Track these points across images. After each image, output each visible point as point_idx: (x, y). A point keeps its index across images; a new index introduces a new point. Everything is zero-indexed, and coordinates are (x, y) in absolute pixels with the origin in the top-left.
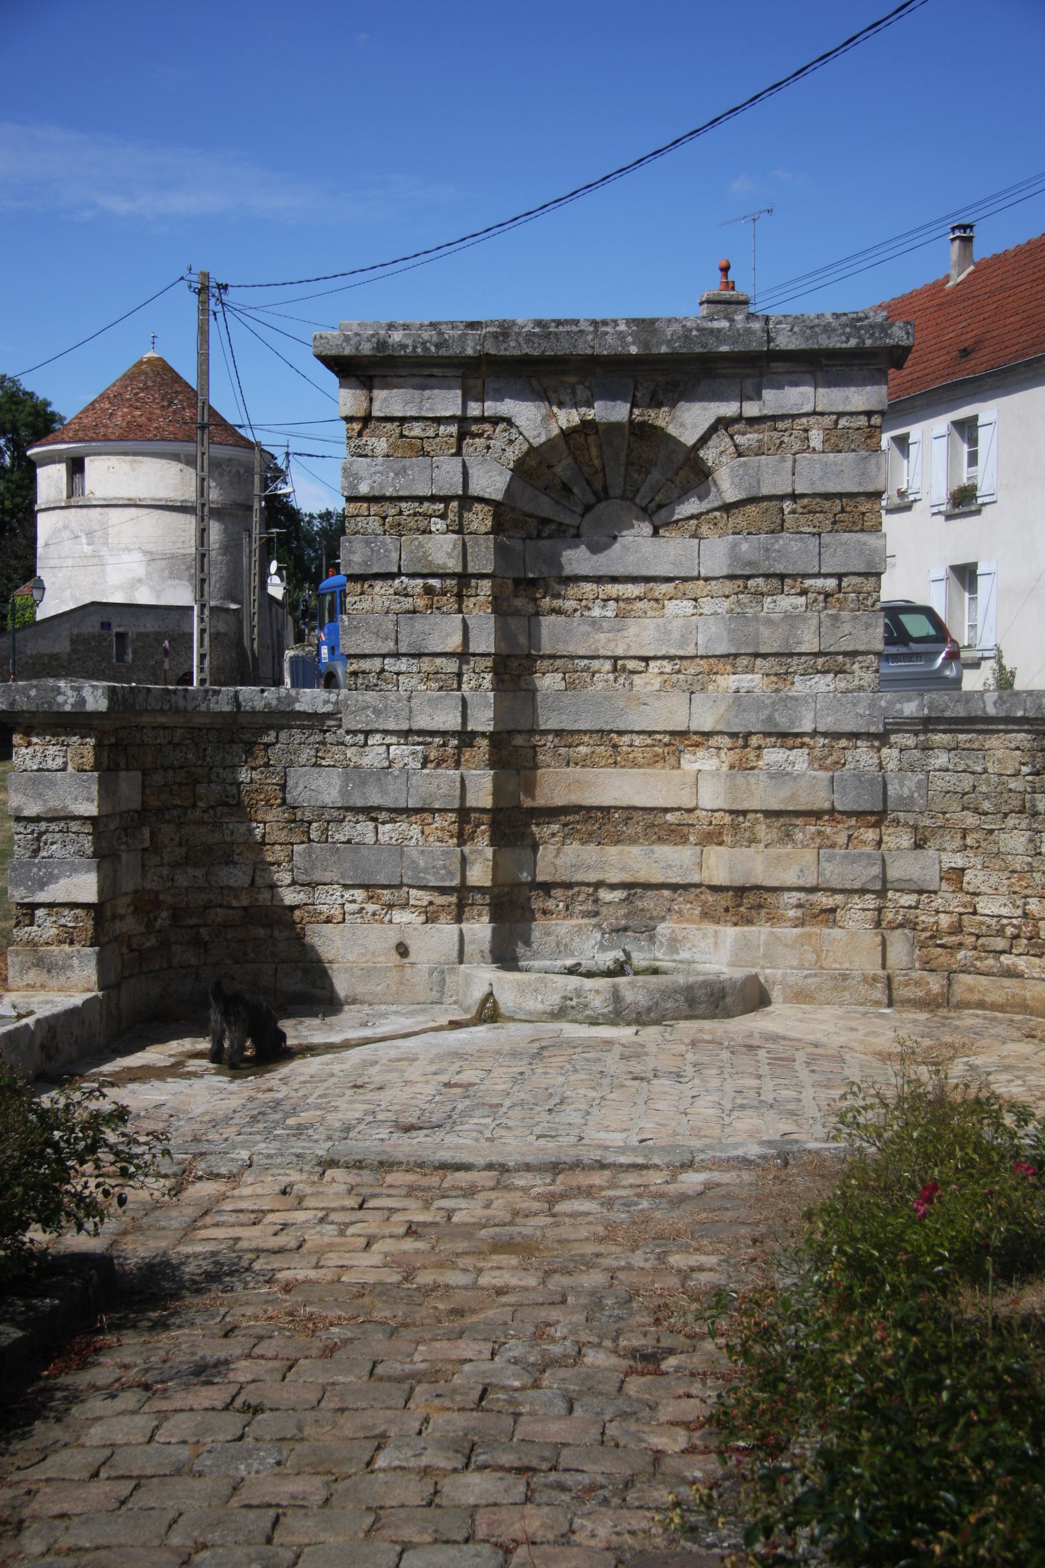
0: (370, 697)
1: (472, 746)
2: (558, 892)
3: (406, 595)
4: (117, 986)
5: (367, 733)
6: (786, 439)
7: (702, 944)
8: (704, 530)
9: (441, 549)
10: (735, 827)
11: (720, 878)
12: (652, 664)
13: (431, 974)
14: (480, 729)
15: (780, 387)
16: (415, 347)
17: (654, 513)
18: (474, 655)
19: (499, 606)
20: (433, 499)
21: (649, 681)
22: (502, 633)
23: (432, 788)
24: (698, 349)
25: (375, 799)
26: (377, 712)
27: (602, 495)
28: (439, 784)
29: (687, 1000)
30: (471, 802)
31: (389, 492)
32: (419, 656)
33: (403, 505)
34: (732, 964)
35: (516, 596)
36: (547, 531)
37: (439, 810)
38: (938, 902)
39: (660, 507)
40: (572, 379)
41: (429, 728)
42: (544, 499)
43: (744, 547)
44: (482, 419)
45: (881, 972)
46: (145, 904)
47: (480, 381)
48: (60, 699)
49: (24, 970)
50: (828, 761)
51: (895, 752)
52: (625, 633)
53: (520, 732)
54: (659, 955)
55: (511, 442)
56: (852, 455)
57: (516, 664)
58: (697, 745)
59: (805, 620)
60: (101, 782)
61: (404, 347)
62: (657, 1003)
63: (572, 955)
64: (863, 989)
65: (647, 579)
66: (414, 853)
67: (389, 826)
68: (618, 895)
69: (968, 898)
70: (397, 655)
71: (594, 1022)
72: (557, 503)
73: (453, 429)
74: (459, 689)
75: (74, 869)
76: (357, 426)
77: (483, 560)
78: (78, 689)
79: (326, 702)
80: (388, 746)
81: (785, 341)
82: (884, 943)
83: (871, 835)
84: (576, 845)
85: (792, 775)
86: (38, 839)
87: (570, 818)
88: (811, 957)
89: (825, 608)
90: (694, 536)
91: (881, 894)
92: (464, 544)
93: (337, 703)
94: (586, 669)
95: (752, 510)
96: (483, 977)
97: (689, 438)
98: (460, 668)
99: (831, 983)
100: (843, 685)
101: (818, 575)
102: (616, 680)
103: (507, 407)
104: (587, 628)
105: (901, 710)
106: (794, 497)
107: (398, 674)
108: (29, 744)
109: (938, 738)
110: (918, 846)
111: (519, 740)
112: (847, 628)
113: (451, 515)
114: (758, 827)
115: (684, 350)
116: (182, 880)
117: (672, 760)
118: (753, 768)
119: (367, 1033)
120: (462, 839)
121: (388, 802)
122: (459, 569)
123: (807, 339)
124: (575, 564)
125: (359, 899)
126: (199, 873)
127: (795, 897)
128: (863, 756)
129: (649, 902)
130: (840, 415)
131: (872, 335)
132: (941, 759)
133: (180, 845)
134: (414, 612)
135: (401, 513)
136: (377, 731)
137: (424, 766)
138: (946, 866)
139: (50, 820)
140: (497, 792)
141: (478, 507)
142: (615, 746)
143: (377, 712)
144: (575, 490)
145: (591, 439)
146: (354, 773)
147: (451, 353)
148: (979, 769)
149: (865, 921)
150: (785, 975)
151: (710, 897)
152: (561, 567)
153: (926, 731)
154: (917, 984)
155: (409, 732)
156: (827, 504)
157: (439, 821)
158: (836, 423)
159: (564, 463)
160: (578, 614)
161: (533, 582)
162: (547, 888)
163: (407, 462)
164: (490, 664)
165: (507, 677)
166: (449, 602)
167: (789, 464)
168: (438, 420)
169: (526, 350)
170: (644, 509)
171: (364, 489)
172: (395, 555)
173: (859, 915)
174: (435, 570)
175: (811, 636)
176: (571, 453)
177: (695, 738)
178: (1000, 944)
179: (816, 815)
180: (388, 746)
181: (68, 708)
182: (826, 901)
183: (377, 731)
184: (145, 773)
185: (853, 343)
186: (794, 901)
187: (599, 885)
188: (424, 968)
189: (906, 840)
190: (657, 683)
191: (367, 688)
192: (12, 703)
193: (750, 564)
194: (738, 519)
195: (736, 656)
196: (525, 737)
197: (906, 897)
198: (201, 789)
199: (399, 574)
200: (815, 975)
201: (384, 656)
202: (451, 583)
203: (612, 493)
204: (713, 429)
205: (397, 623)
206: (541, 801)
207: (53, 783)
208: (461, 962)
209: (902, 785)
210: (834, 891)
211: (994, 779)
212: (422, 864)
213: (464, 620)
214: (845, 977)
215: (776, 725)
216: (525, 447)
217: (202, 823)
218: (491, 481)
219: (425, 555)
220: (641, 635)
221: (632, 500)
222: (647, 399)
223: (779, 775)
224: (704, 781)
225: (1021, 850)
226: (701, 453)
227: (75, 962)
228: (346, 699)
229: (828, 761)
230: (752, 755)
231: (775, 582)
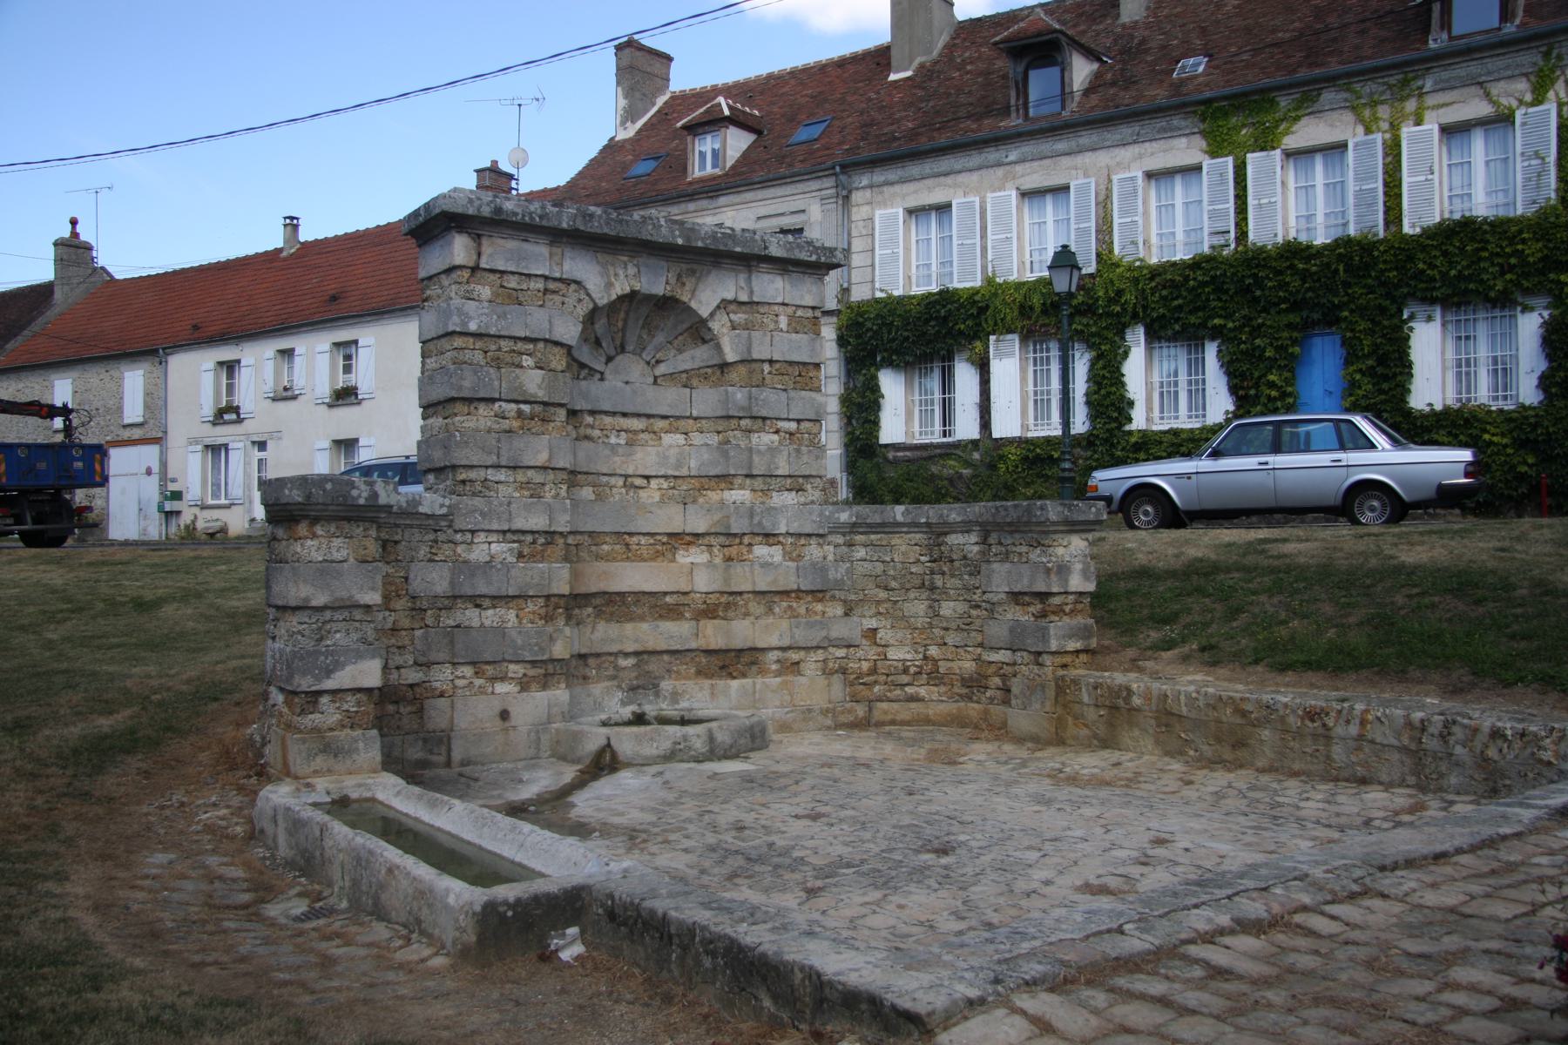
0: (478, 502)
2: (591, 661)
5: (473, 532)
9: (533, 381)
11: (717, 642)
12: (654, 483)
14: (560, 529)
20: (526, 339)
21: (651, 495)
25: (483, 589)
31: (493, 331)
32: (515, 468)
33: (503, 343)
38: (860, 653)
39: (658, 362)
48: (355, 493)
49: (311, 756)
51: (831, 548)
58: (689, 544)
61: (516, 214)
65: (649, 416)
66: (514, 634)
67: (490, 612)
68: (630, 662)
70: (497, 467)
75: (359, 656)
79: (442, 506)
85: (768, 565)
87: (598, 601)
88: (788, 698)
100: (802, 500)
101: (789, 420)
104: (607, 452)
106: (771, 362)
108: (314, 536)
109: (859, 538)
112: (805, 458)
117: (670, 556)
121: (491, 591)
128: (814, 551)
129: (654, 666)
132: (861, 553)
135: (499, 349)
142: (627, 545)
143: (483, 514)
154: (849, 712)
156: (790, 370)
157: (531, 606)
163: (508, 308)
168: (529, 276)
169: (606, 230)
173: (813, 666)
181: (362, 501)
182: (794, 656)
185: (814, 258)
187: (616, 655)
188: (523, 729)
189: (839, 611)
190: (657, 497)
191: (474, 494)
192: (309, 497)
193: (743, 408)
202: (538, 408)
204: (718, 307)
210: (800, 648)
211: (899, 566)
212: (519, 642)
214: (810, 711)
216: (591, 306)
219: (521, 386)
220: (646, 459)
224: (696, 571)
227: (361, 745)
230: (745, 550)
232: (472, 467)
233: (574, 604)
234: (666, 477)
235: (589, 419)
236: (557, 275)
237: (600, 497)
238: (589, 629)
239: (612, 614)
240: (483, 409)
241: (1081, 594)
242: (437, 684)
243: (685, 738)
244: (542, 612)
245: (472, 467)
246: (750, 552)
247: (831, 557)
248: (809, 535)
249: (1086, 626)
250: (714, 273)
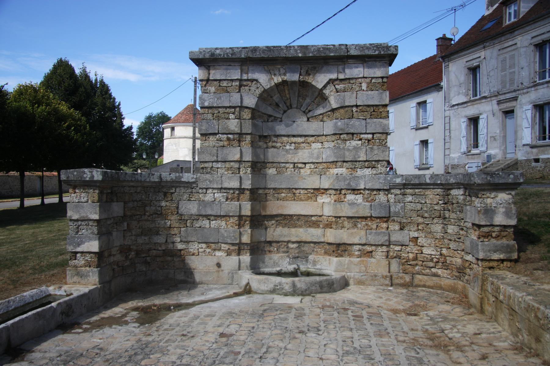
0: (208, 176)
1: (243, 193)
2: (274, 244)
3: (221, 141)
4: (110, 282)
5: (207, 189)
6: (354, 86)
7: (325, 263)
8: (325, 119)
9: (233, 124)
10: (337, 222)
11: (331, 240)
13: (229, 274)
14: (246, 187)
15: (351, 68)
16: (224, 55)
17: (307, 113)
18: (244, 161)
19: (253, 144)
20: (230, 107)
21: (306, 171)
22: (255, 154)
23: (229, 208)
24: (323, 55)
25: (209, 212)
26: (210, 182)
27: (290, 107)
28: (232, 207)
29: (320, 286)
30: (243, 213)
31: (215, 105)
32: (225, 162)
33: (220, 110)
34: (335, 271)
35: (260, 141)
36: (270, 119)
37: (232, 216)
38: (408, 249)
39: (310, 111)
40: (279, 67)
41: (228, 187)
42: (269, 108)
43: (339, 124)
44: (248, 80)
45: (388, 274)
46: (125, 250)
47: (247, 67)
48: (85, 176)
49: (72, 276)
50: (370, 199)
51: (393, 196)
52: (298, 155)
53: (261, 189)
54: (310, 267)
55: (258, 88)
56: (377, 92)
57: (259, 165)
58: (323, 193)
59: (361, 149)
60: (100, 207)
62: (309, 288)
63: (279, 266)
64: (382, 280)
65: (306, 136)
66: (223, 231)
67: (214, 222)
68: (295, 245)
69: (419, 248)
70: (217, 162)
71: (286, 295)
72: (274, 110)
73: (237, 83)
74: (239, 173)
75: (90, 239)
76: (204, 83)
77: (248, 128)
78: (91, 172)
79: (193, 178)
80: (214, 193)
81: (353, 52)
82: (389, 264)
83: (384, 225)
84: (281, 228)
85: (357, 204)
86: (78, 228)
87: (279, 219)
88: (364, 269)
89: (368, 145)
90: (322, 121)
91: (388, 246)
92: (241, 123)
93: (196, 178)
94: (284, 167)
95: (342, 111)
96: (247, 276)
97: (320, 86)
98: (239, 166)
99: (371, 278)
100: (375, 172)
102: (294, 171)
103: (256, 76)
104: (284, 153)
105: (395, 181)
106: (357, 106)
107: (218, 168)
108: (75, 193)
109: (408, 191)
110: (402, 229)
111: (261, 192)
112: (376, 152)
113: (236, 113)
114: (345, 222)
115: (318, 55)
116: (140, 240)
118: (343, 201)
119: (203, 298)
120: (240, 226)
122: (239, 132)
123: (361, 51)
124: (280, 131)
125: (204, 247)
126: (146, 238)
127: (357, 247)
128: (382, 197)
129: (306, 248)
130: (372, 78)
131: (383, 50)
132: (410, 198)
133: (139, 228)
134: (224, 146)
135: (219, 112)
136: (210, 188)
137: (226, 200)
138: (411, 236)
139: (82, 221)
140: (252, 210)
141: (246, 110)
142: (294, 194)
143: (210, 182)
144: (280, 105)
145: (286, 87)
146: (203, 203)
147: (236, 57)
148: (423, 202)
149: (382, 256)
150: (354, 275)
151: (327, 247)
152: (275, 131)
153: (404, 188)
154: (401, 278)
155: (221, 188)
156: (368, 109)
157: (232, 220)
158: (371, 81)
159: (276, 96)
161: (266, 137)
162: (270, 243)
163: (221, 95)
164: (250, 165)
165: (256, 169)
166: (236, 143)
167: (355, 95)
168: (232, 80)
169: (263, 55)
170: (304, 112)
171: (206, 104)
172: (217, 127)
173: (380, 254)
174: (231, 132)
175: (363, 155)
176: (279, 92)
177: (322, 191)
178: (431, 264)
179: (365, 218)
180: (214, 193)
181: (88, 179)
182: (369, 249)
183: (210, 188)
184: (125, 203)
185: (377, 53)
186: (357, 249)
187: (288, 242)
188: (226, 272)
189: (397, 227)
190: (309, 172)
191: (207, 173)
192: (68, 177)
193: (341, 129)
194: (337, 114)
195: (337, 162)
196: (263, 190)
197: (397, 247)
198: (148, 208)
199: (218, 133)
200: (365, 275)
201: (213, 162)
202: (236, 136)
203: (293, 106)
204: (328, 83)
205: (217, 150)
206: (268, 213)
207: (83, 207)
208: (239, 270)
209: (396, 208)
210: (372, 245)
212: (226, 235)
213: (241, 149)
214: (376, 276)
215: (351, 186)
216: (263, 89)
217: (147, 220)
218: (250, 101)
220: (303, 155)
221: (300, 109)
222: (305, 73)
223: (352, 204)
224: (325, 206)
225: (439, 231)
226: (324, 91)
227: (91, 274)
228: (199, 177)
229: (370, 199)
230: (343, 197)
231: (350, 136)
232: (206, 162)
234: (313, 163)
235: (275, 139)
236: (246, 78)
237: (279, 173)
238: (272, 229)
239: (286, 224)
240: (211, 138)
241: (505, 226)
242: (192, 250)
243: (280, 284)
244: (237, 222)
245: (206, 162)
246: (345, 197)
247: (392, 201)
248: (379, 190)
249: (508, 246)
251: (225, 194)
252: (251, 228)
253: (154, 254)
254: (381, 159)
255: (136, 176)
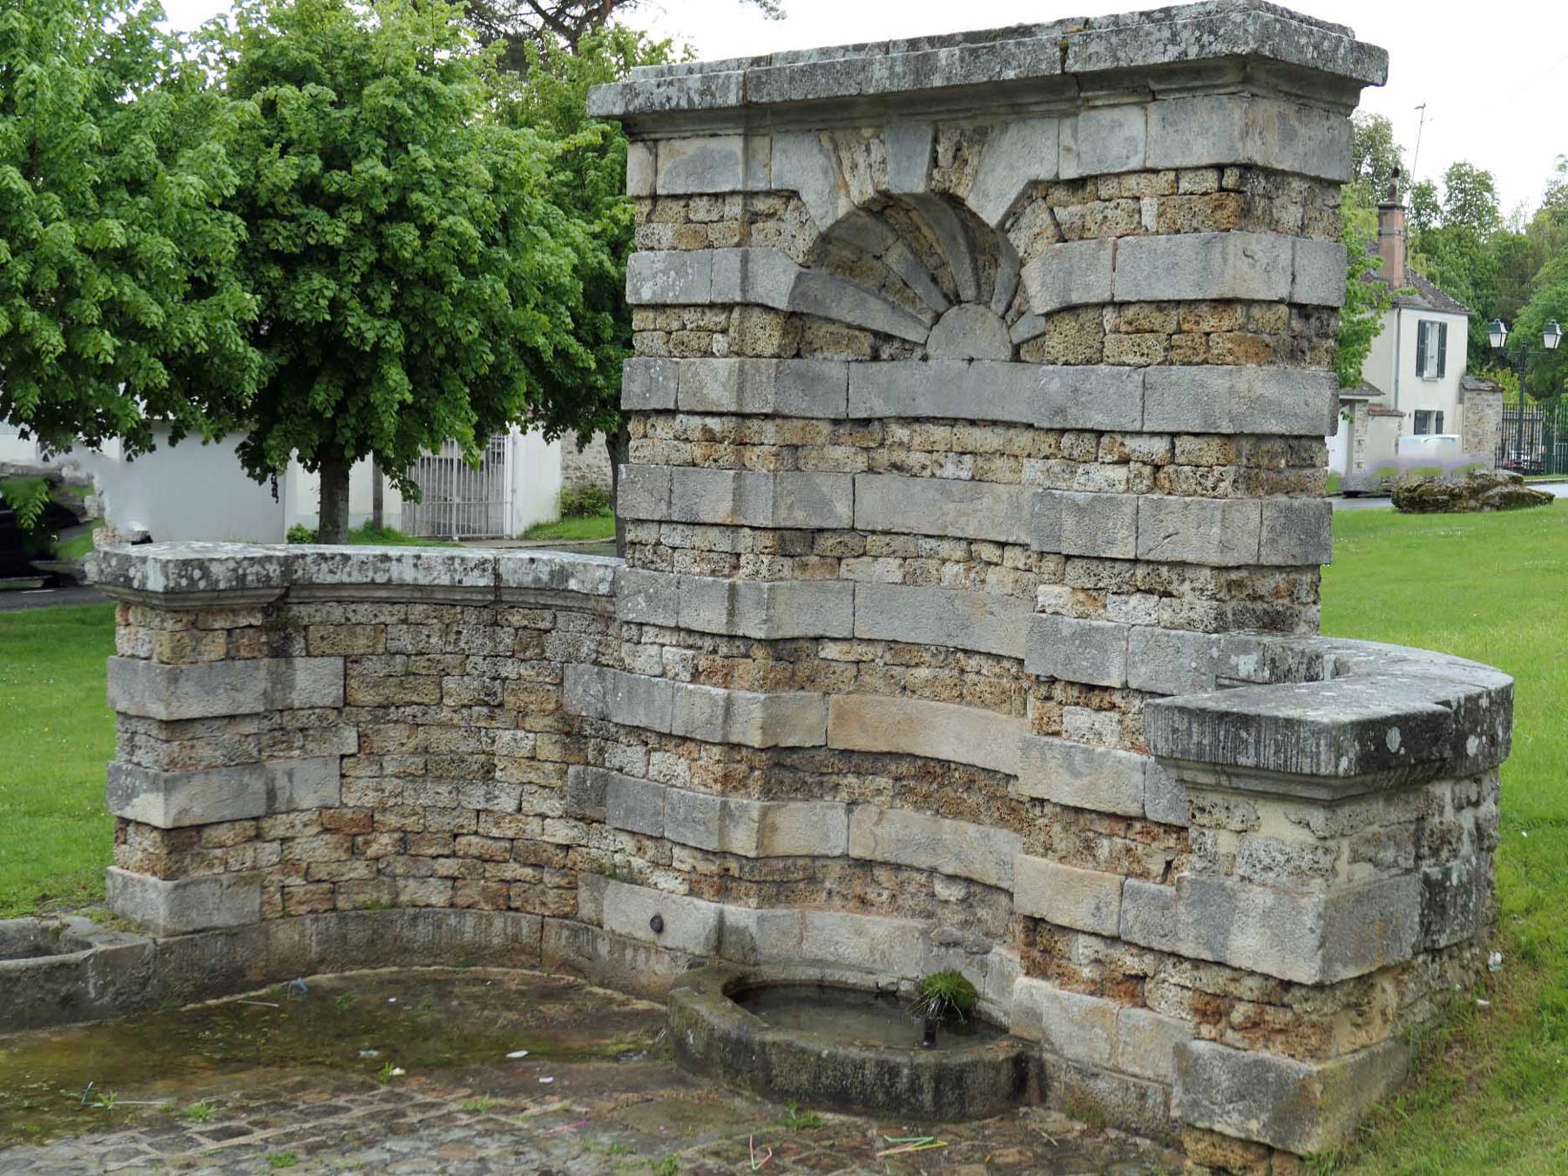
6: (1109, 213)
12: (1009, 553)
20: (712, 306)
33: (687, 316)
40: (867, 132)
47: (767, 139)
84: (908, 810)
87: (904, 768)
89: (1150, 490)
100: (1166, 616)
101: (1140, 433)
107: (674, 549)
120: (728, 782)
133: (415, 752)
135: (684, 327)
156: (1157, 319)
160: (928, 473)
166: (725, 450)
167: (1106, 255)
173: (1173, 994)
175: (1123, 533)
182: (1132, 963)
187: (932, 872)
193: (1061, 411)
196: (845, 647)
198: (450, 683)
222: (950, 154)
231: (1089, 442)
233: (787, 769)
235: (900, 433)
244: (719, 770)
250: (1013, 133)
251: (690, 653)
252: (767, 792)
253: (473, 851)
254: (1190, 558)
255: (394, 566)
